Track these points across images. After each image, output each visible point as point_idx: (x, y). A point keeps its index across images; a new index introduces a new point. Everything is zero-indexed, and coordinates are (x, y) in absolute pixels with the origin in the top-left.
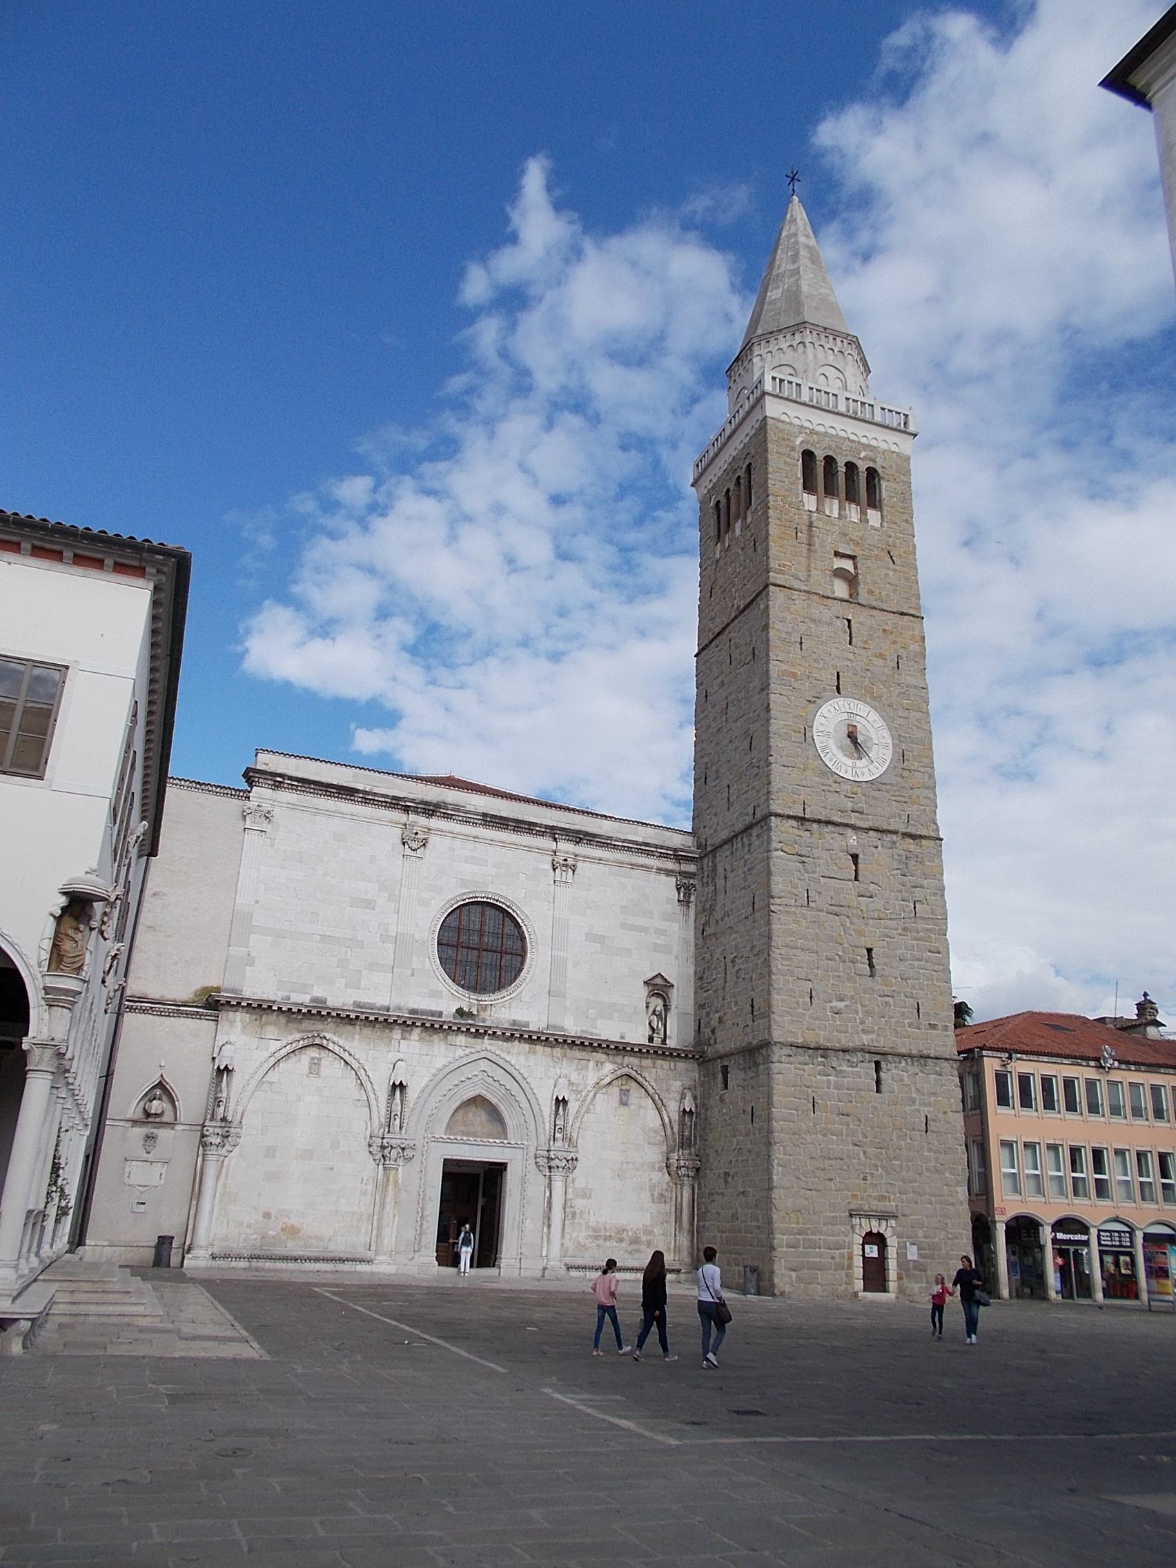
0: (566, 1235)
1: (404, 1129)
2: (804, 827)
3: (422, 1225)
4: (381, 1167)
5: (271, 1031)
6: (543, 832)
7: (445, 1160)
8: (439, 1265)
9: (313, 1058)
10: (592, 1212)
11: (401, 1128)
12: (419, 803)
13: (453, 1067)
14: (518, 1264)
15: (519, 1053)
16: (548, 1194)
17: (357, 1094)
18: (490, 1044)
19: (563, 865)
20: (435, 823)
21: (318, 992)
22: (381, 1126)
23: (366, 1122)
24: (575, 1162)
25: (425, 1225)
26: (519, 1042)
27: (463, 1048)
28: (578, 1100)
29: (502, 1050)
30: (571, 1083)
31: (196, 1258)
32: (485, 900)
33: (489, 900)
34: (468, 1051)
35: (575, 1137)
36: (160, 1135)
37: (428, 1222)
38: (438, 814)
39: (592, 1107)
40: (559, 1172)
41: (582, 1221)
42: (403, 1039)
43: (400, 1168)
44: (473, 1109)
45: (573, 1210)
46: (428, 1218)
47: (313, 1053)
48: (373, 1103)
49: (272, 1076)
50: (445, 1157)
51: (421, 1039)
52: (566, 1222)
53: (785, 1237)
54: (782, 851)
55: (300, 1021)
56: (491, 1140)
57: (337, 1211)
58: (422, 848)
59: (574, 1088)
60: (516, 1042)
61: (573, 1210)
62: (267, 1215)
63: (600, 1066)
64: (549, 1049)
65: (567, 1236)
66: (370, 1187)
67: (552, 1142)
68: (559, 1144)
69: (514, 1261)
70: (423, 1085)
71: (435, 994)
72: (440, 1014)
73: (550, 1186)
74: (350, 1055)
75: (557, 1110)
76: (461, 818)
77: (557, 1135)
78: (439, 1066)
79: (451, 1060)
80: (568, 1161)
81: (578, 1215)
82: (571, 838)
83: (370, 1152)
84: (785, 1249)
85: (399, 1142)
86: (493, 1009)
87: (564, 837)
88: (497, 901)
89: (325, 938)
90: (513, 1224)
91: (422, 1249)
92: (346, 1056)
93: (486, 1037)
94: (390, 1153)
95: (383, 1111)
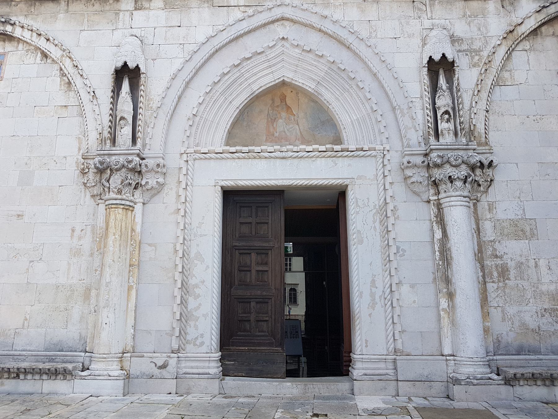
0: (492, 310)
3: (183, 303)
4: (102, 207)
7: (222, 187)
8: (226, 373)
10: (542, 263)
14: (391, 372)
16: (438, 234)
17: (60, 98)
22: (102, 141)
23: (80, 143)
24: (489, 172)
25: (192, 303)
27: (242, 9)
34: (250, 11)
35: (480, 127)
37: (197, 297)
39: (506, 75)
40: (456, 190)
41: (525, 284)
42: (136, 9)
43: (138, 208)
44: (284, 114)
45: (499, 262)
46: (197, 291)
48: (88, 107)
50: (224, 184)
52: (490, 286)
57: (28, 283)
59: (464, 47)
61: (499, 262)
63: (509, 8)
65: (496, 314)
66: (87, 243)
67: (432, 139)
68: (447, 139)
69: (382, 365)
70: (174, 70)
73: (441, 220)
74: (48, 40)
75: (434, 88)
77: (442, 126)
78: (202, 39)
80: (473, 168)
83: (85, 184)
85: (122, 159)
90: (372, 295)
91: (189, 347)
92: (42, 43)
94: (108, 181)
95: (106, 120)
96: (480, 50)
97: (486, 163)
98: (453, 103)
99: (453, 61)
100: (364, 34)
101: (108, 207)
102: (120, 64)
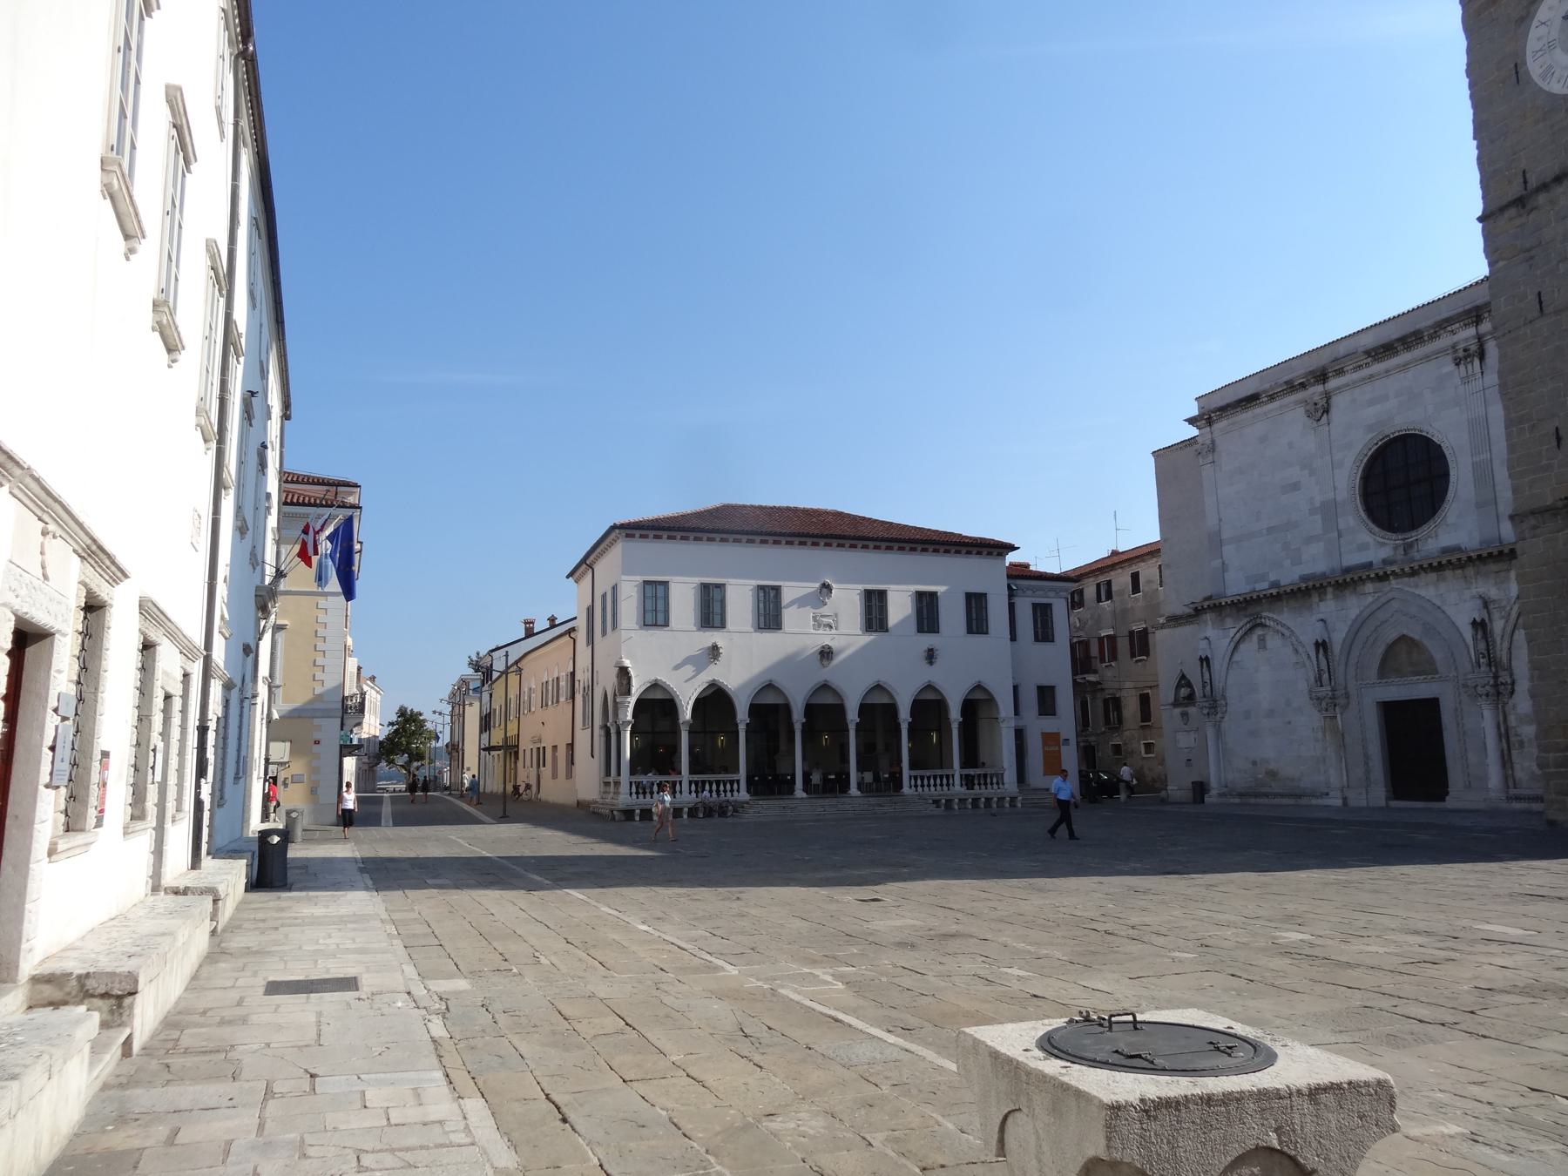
1: (1333, 681)
2: (1529, 207)
5: (1229, 622)
6: (1435, 332)
9: (1259, 636)
11: (1330, 679)
12: (1306, 377)
13: (1366, 614)
15: (1427, 585)
18: (1397, 584)
19: (1466, 358)
20: (1333, 383)
21: (1272, 577)
26: (1426, 573)
28: (1502, 618)
29: (1410, 586)
30: (1486, 603)
31: (1210, 797)
32: (1397, 434)
33: (1401, 433)
34: (1377, 595)
35: (1505, 659)
36: (1189, 711)
38: (1330, 374)
43: (1339, 716)
47: (1259, 632)
49: (1237, 657)
51: (1336, 597)
52: (1514, 752)
53: (1551, 755)
54: (1502, 259)
55: (1245, 609)
56: (1415, 678)
58: (1325, 415)
59: (1496, 606)
60: (1423, 574)
61: (1519, 738)
62: (1254, 763)
64: (1459, 572)
66: (1320, 735)
71: (1363, 547)
72: (1369, 565)
76: (1351, 367)
77: (1482, 660)
78: (1353, 617)
79: (1362, 608)
81: (1526, 745)
82: (1466, 322)
84: (1552, 770)
86: (1420, 543)
87: (1457, 325)
88: (1408, 430)
89: (1270, 530)
92: (1279, 628)
93: (1391, 577)
95: (1316, 669)
96: (1505, 607)
97: (1503, 681)
98: (1488, 644)
99: (1483, 620)
100: (1439, 604)
101: (1325, 718)
102: (1314, 641)
